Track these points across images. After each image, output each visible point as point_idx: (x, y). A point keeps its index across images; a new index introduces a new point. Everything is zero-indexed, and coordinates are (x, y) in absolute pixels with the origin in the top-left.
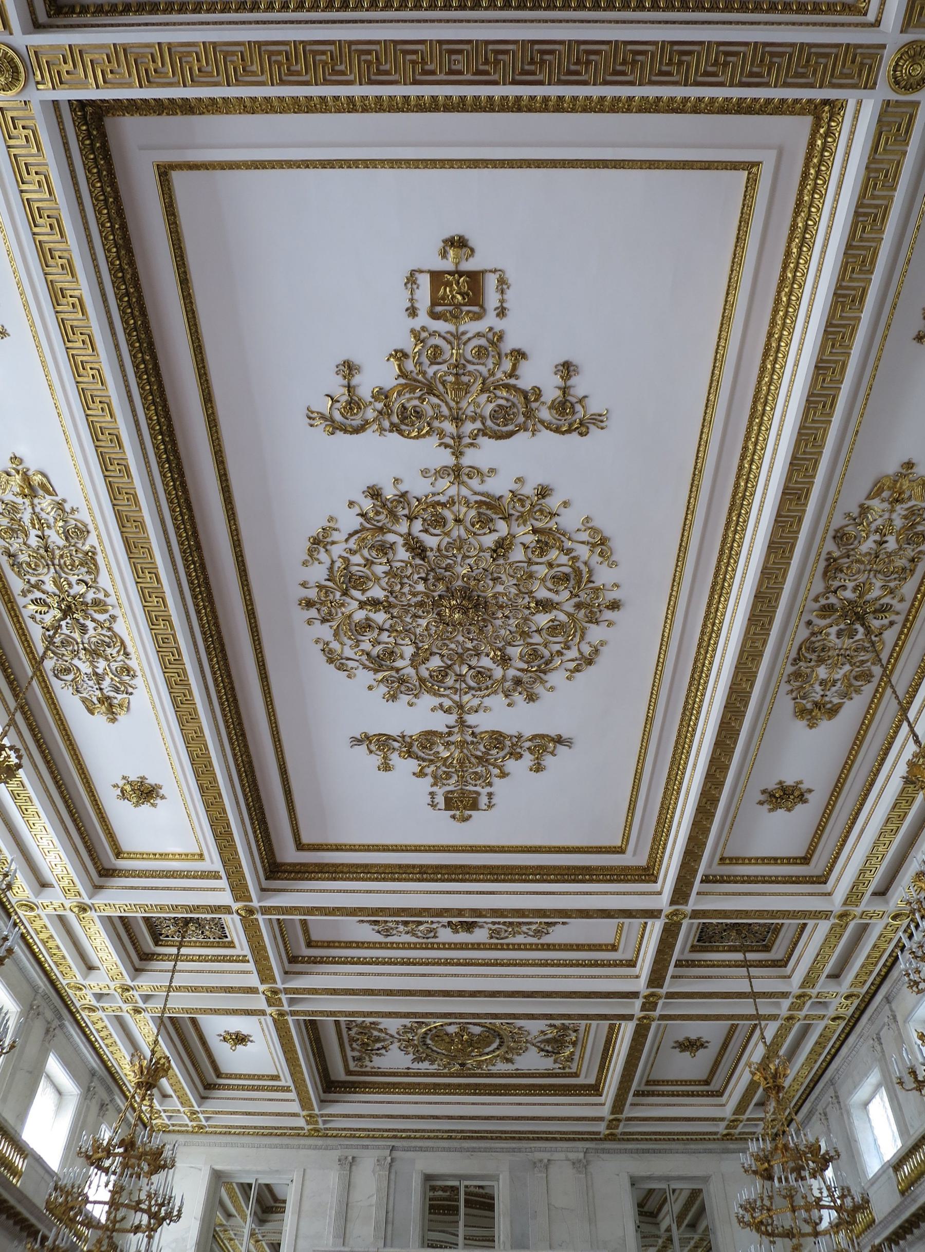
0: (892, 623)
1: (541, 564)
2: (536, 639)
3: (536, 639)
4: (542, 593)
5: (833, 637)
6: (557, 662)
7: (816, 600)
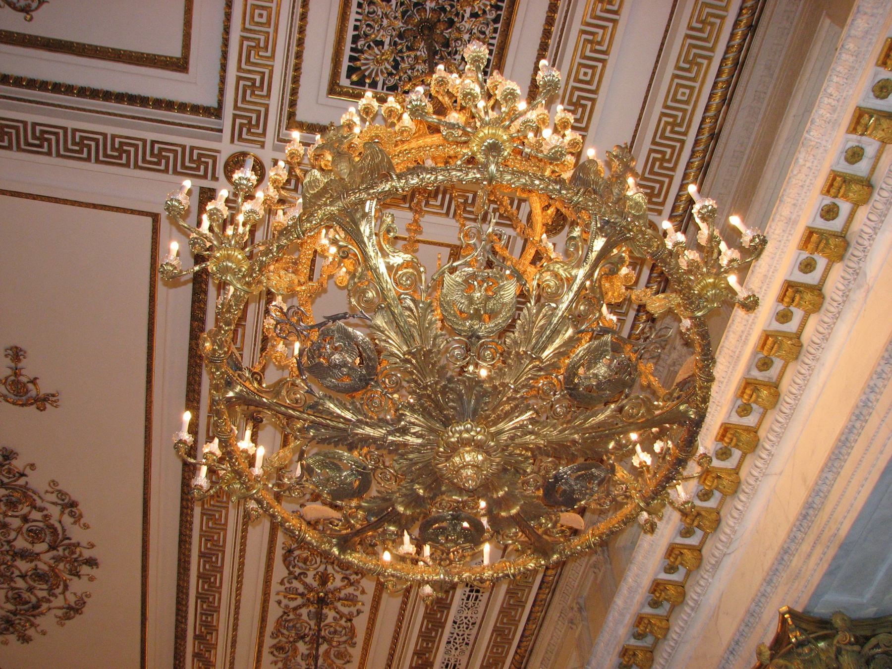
0: (359, 612)
1: (17, 517)
2: (20, 583)
3: (20, 583)
4: (21, 543)
5: (305, 617)
6: (45, 606)
7: (282, 583)
